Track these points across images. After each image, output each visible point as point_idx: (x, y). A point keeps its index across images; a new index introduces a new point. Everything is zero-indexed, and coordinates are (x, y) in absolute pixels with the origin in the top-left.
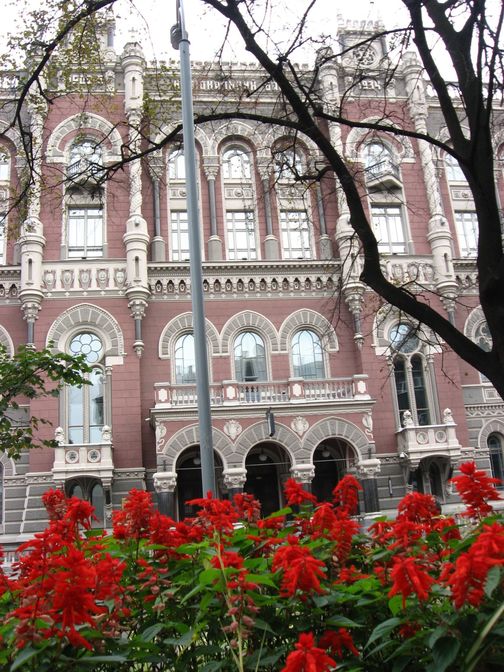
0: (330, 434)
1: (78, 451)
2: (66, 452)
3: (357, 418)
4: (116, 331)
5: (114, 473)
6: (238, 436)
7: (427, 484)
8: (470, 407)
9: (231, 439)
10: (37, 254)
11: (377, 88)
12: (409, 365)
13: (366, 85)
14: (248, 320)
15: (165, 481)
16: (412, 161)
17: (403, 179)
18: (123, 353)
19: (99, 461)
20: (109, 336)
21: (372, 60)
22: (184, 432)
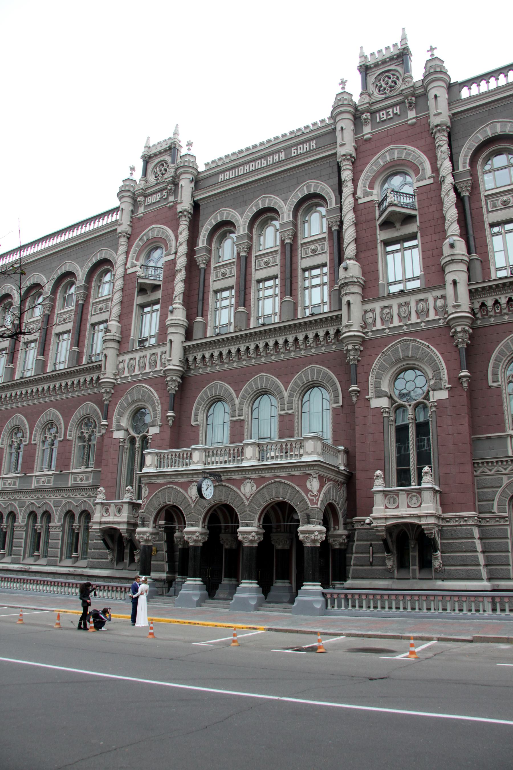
0: (274, 496)
1: (110, 506)
2: (103, 506)
3: (302, 480)
7: (414, 554)
8: (487, 463)
9: (192, 500)
10: (110, 349)
11: (396, 114)
14: (262, 384)
16: (431, 181)
17: (418, 205)
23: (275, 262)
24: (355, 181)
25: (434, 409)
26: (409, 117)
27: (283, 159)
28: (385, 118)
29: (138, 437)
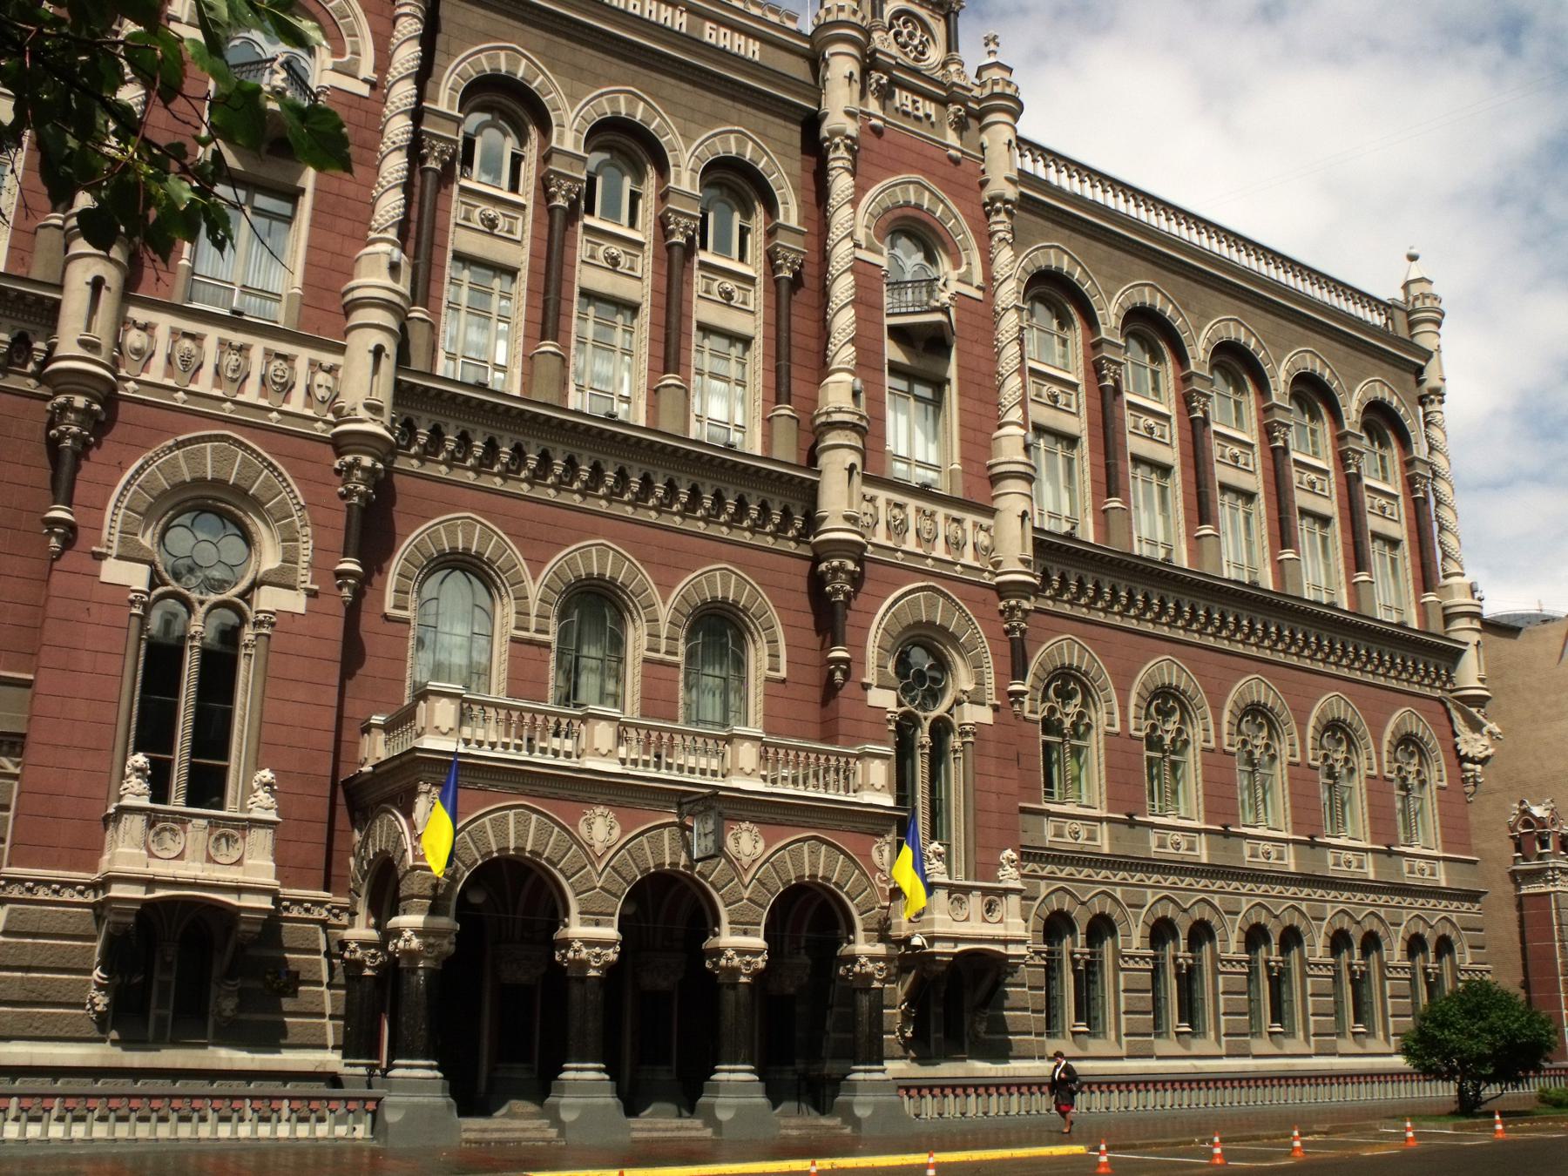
4: (298, 524)
5: (277, 900)
6: (608, 848)
12: (923, 736)
13: (909, 102)
15: (431, 940)
16: (979, 295)
18: (308, 585)
19: (239, 862)
20: (277, 534)
21: (923, 53)
22: (486, 819)
23: (631, 269)
24: (854, 203)
25: (970, 739)
26: (948, 142)
27: (684, 30)
28: (909, 109)
29: (202, 603)
